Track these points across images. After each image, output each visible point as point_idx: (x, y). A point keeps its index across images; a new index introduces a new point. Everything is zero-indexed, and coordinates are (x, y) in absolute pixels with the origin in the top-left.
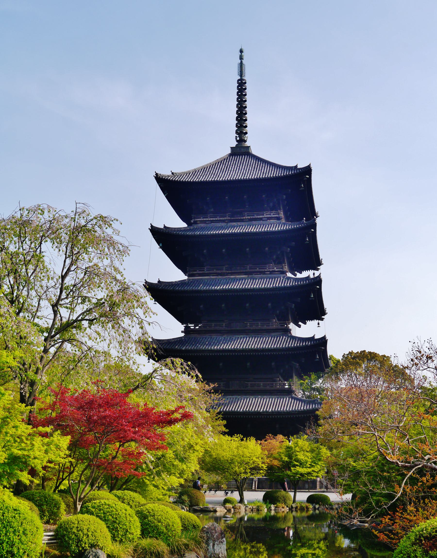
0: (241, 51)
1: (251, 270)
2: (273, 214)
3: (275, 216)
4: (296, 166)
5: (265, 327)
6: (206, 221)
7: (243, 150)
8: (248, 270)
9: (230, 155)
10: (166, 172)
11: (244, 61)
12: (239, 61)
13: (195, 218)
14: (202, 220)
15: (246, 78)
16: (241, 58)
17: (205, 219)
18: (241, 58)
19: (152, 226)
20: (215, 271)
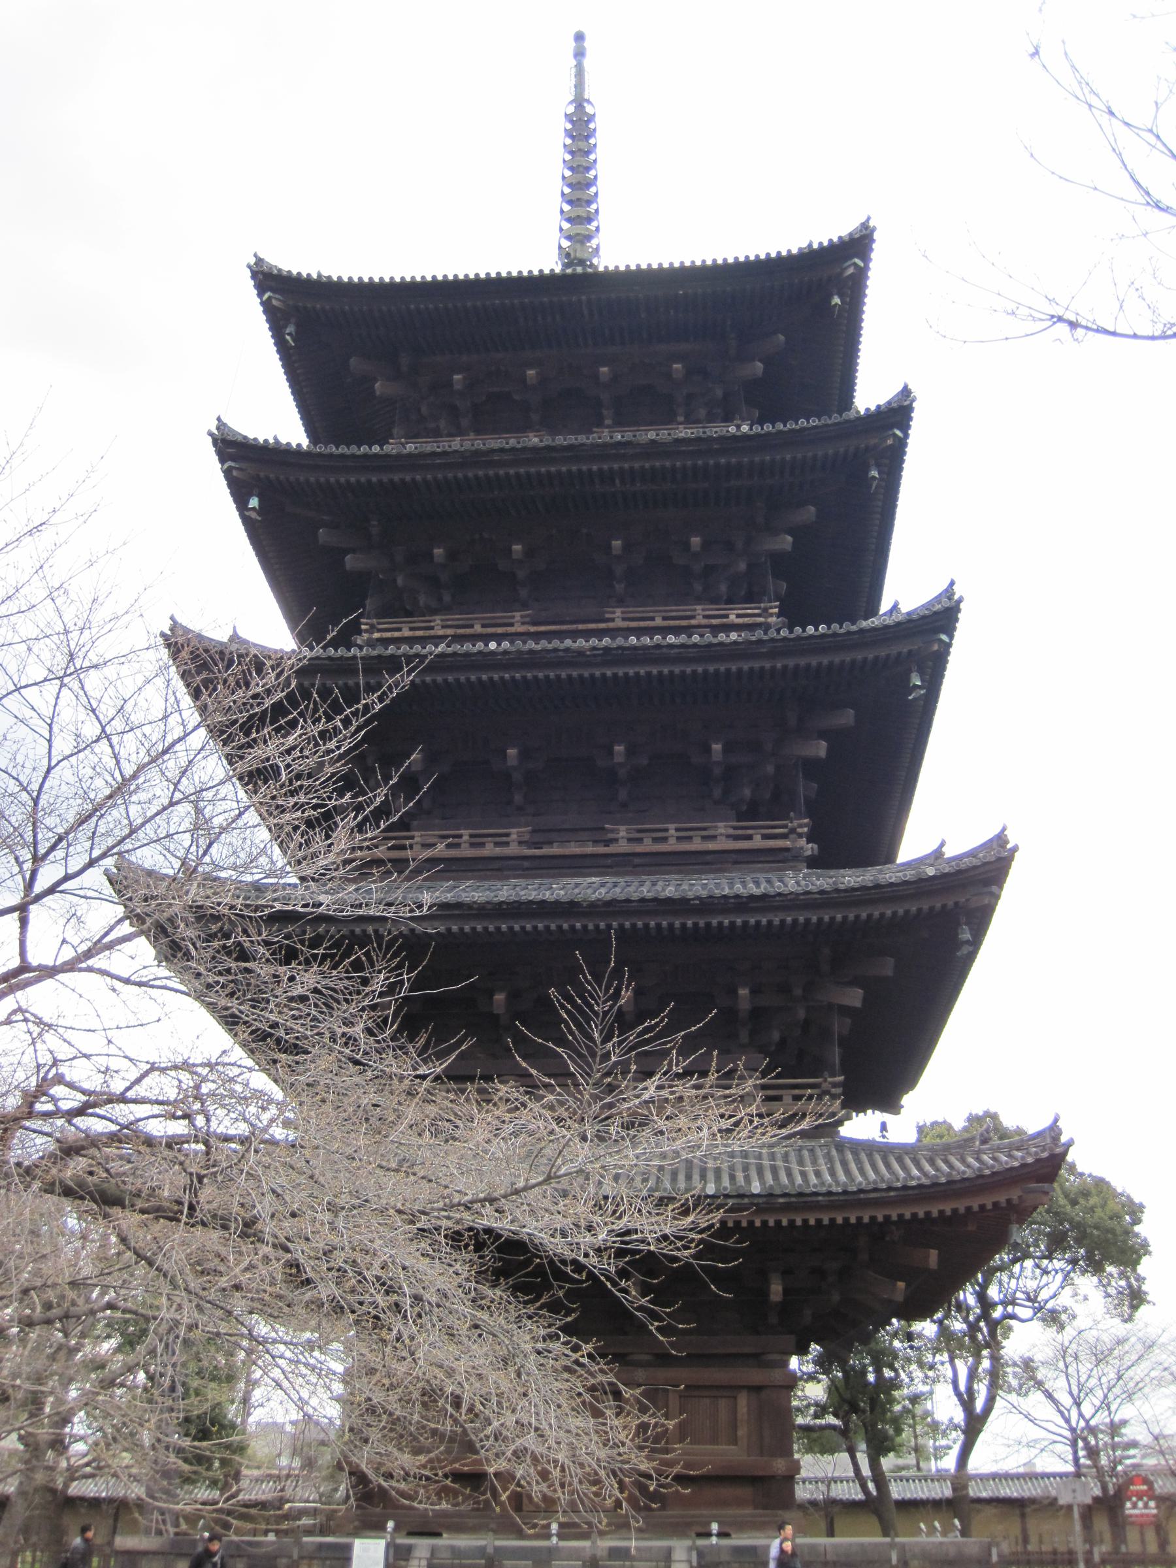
0: (579, 37)
5: (697, 845)
18: (579, 54)
19: (221, 425)
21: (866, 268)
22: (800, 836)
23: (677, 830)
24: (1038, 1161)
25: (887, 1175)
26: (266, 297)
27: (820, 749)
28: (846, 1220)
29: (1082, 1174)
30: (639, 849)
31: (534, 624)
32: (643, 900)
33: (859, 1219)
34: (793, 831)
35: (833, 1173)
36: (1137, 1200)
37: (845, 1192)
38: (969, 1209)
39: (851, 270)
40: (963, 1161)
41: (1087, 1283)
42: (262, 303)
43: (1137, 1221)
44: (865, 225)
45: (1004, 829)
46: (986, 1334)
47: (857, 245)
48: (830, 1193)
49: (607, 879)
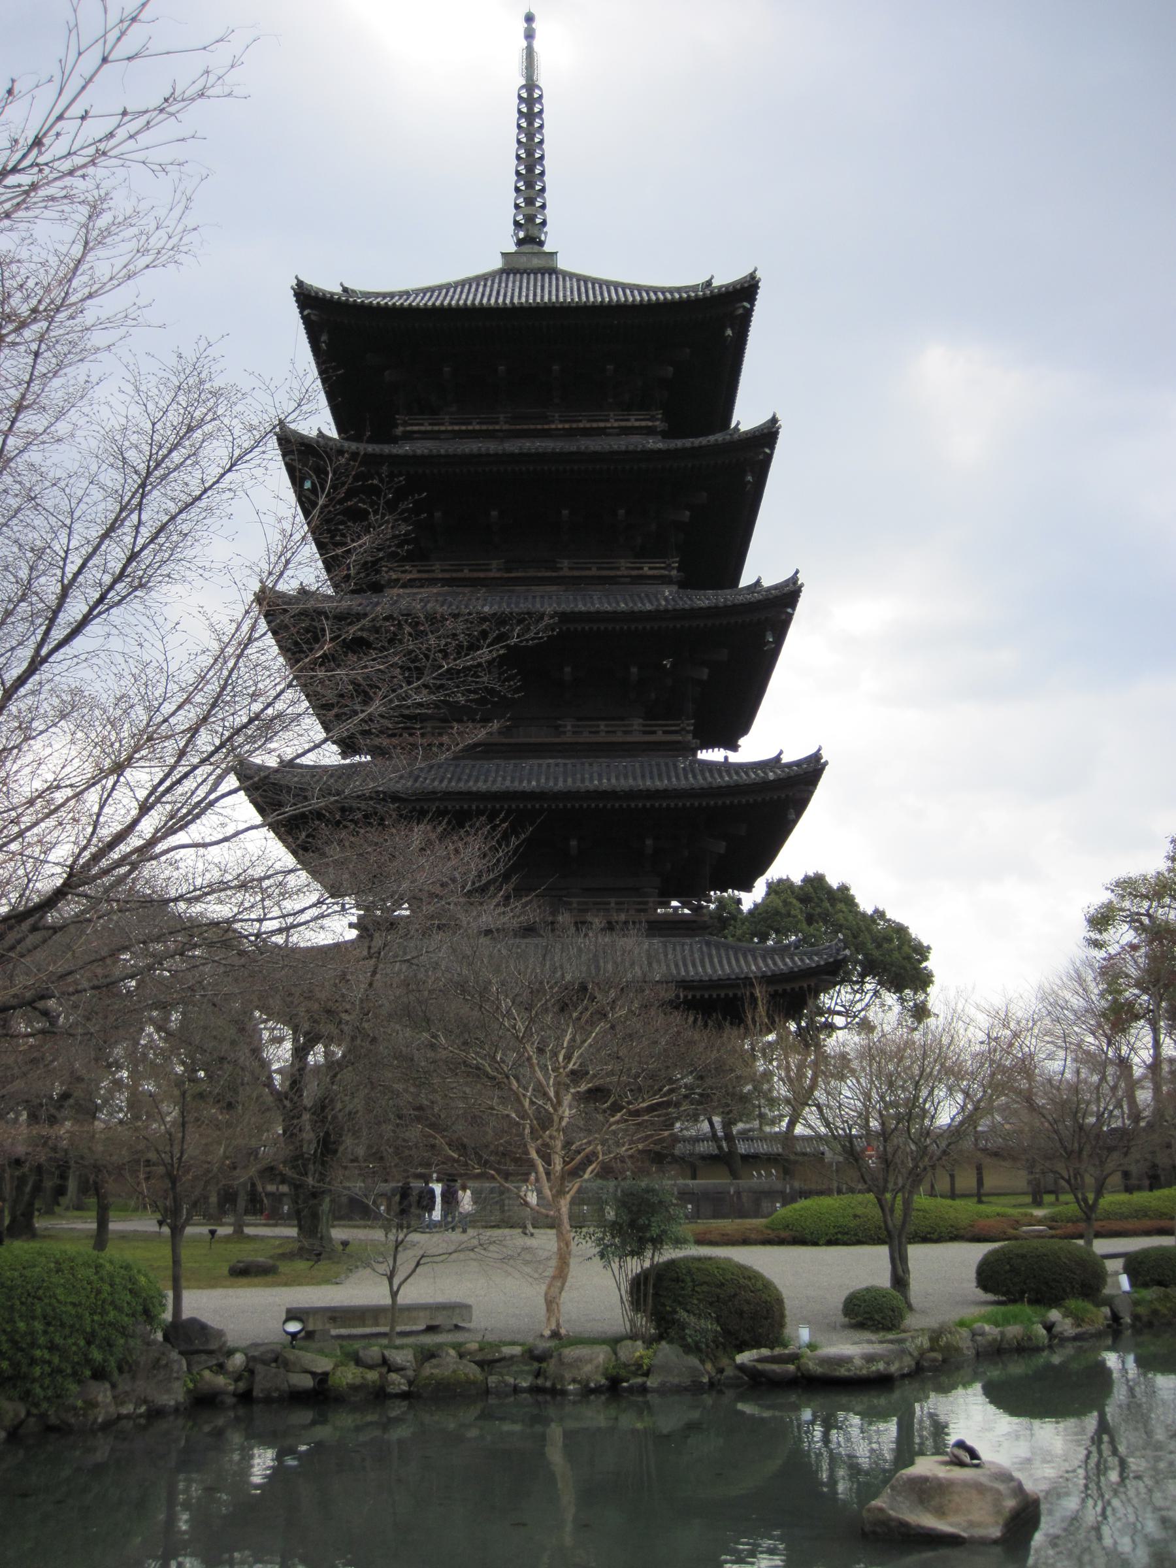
0: (529, 18)
1: (576, 573)
2: (637, 420)
3: (643, 424)
4: (709, 283)
5: (619, 738)
6: (439, 432)
7: (536, 262)
8: (566, 572)
9: (502, 271)
10: (328, 283)
11: (536, 44)
12: (525, 44)
13: (405, 424)
14: (429, 428)
15: (543, 78)
16: (529, 35)
17: (436, 428)
18: (529, 35)
20: (466, 573)
21: (751, 310)
22: (688, 732)
23: (606, 726)
24: (827, 964)
25: (737, 970)
26: (306, 313)
27: (704, 674)
28: (710, 996)
29: (889, 920)
30: (581, 740)
31: (508, 570)
32: (588, 791)
33: (718, 995)
34: (683, 729)
35: (703, 966)
36: (925, 944)
37: (710, 980)
38: (785, 990)
39: (741, 311)
40: (783, 960)
41: (890, 998)
42: (303, 317)
43: (926, 959)
44: (752, 276)
45: (819, 750)
46: (810, 1038)
47: (747, 290)
48: (701, 981)
49: (559, 761)
